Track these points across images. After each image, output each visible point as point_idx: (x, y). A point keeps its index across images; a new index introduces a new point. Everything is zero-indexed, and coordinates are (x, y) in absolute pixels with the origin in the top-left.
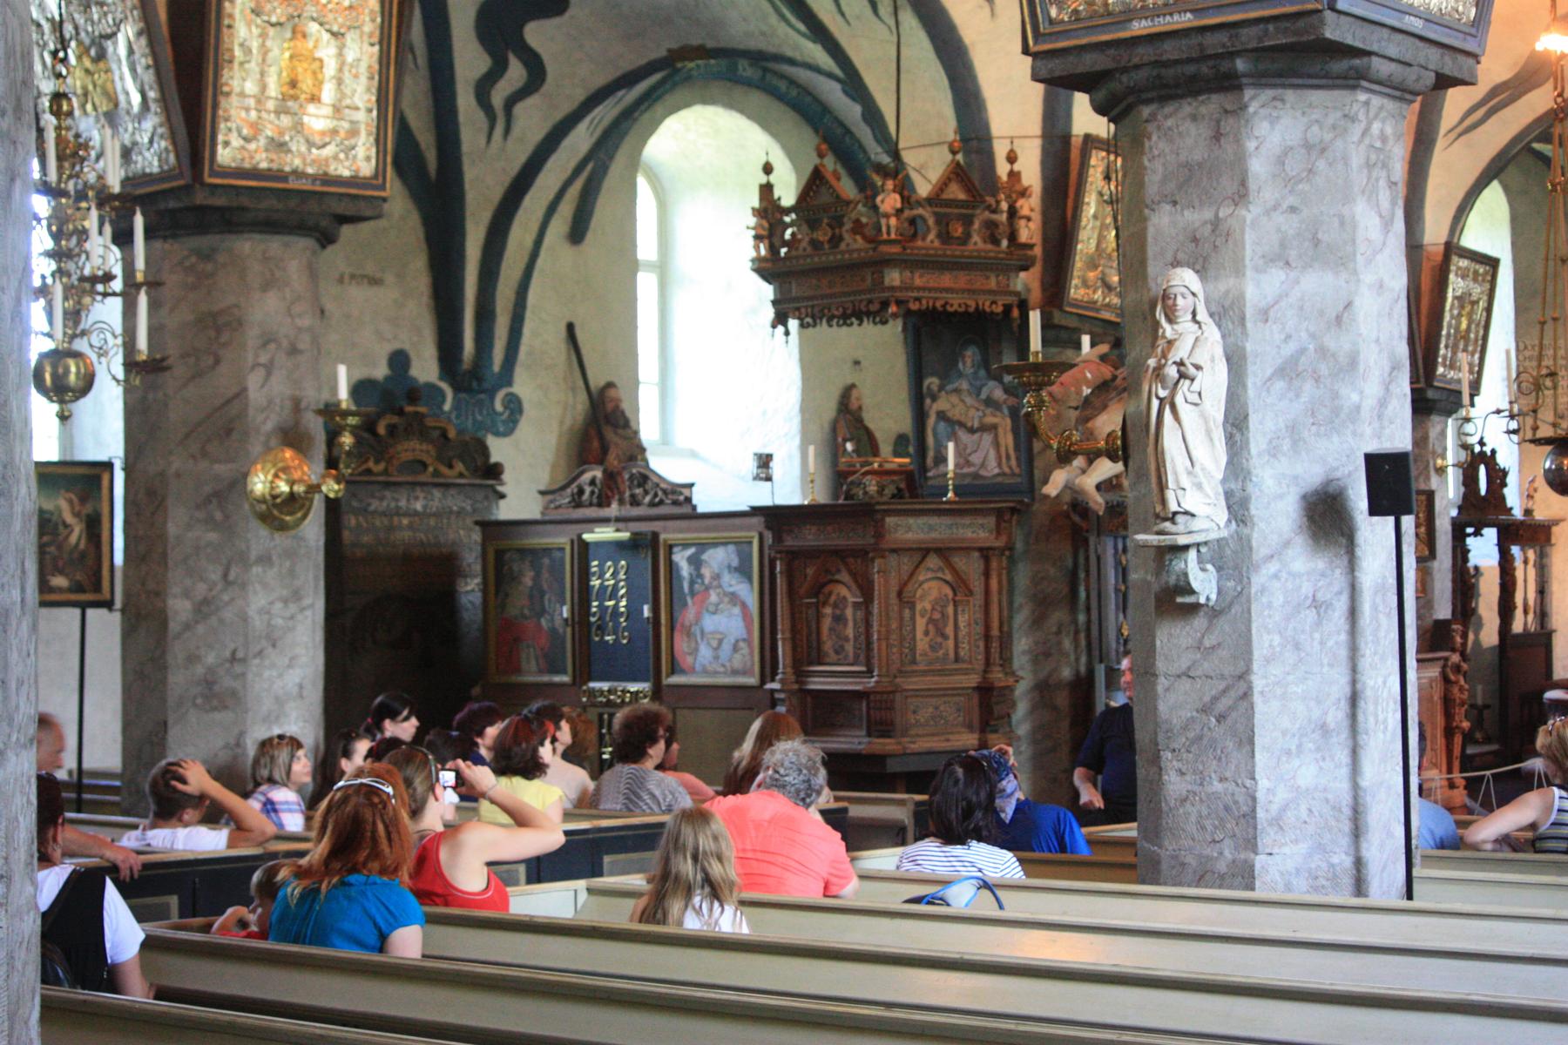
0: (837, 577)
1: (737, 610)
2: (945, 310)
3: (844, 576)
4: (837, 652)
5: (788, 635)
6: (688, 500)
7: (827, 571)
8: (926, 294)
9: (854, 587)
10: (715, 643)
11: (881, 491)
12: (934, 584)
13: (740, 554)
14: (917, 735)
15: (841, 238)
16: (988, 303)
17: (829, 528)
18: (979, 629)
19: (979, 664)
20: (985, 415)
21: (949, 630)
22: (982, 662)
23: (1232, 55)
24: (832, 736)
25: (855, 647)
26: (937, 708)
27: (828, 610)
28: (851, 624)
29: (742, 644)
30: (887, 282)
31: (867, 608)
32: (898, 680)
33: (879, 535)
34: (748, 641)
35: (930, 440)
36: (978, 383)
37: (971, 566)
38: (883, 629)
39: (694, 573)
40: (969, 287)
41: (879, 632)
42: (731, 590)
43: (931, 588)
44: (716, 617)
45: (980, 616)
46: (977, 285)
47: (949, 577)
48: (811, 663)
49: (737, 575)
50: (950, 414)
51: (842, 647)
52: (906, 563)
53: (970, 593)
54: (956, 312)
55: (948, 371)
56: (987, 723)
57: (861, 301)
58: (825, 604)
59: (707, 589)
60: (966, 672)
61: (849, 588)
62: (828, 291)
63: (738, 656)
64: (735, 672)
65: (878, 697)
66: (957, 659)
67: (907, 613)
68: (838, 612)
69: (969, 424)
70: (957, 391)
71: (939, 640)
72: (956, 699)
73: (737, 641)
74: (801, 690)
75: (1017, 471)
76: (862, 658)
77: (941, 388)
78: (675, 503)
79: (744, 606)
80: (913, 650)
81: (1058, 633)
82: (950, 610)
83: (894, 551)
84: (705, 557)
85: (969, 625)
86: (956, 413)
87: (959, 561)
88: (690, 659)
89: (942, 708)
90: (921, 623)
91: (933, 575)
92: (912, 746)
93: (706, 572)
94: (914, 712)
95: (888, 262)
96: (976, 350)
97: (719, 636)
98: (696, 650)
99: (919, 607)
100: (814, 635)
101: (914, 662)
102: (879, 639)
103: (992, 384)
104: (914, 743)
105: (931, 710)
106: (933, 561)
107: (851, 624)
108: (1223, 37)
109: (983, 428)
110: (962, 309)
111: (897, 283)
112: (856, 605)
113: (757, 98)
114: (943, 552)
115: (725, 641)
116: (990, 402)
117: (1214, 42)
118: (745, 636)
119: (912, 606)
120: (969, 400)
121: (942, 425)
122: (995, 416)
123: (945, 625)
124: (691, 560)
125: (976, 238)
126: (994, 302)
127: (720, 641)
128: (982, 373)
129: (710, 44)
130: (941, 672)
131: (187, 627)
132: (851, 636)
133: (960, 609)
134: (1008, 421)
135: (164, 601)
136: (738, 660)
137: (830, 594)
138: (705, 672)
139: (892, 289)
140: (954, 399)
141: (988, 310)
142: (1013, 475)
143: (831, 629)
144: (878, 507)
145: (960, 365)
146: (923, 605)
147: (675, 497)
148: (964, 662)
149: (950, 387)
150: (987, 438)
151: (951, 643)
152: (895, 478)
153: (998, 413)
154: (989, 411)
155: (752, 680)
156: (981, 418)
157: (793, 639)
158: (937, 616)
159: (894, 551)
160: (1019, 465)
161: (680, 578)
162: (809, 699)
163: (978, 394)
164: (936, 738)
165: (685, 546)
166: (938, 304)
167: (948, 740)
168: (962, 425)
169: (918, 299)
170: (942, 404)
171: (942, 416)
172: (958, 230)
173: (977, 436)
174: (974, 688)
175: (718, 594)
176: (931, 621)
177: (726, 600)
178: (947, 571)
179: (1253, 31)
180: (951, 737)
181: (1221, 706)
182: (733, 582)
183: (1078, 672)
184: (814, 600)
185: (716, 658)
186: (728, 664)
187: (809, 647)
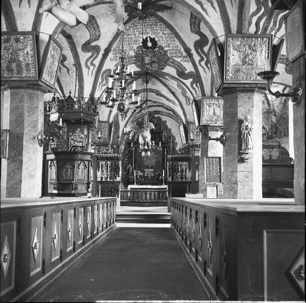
3: (69, 164)
23: (255, 87)
33: (77, 157)
35: (70, 143)
37: (86, 163)
43: (82, 166)
52: (79, 162)
55: (74, 132)
95: (82, 112)
108: (255, 85)
109: (80, 142)
112: (71, 169)
114: (84, 161)
116: (81, 137)
117: (253, 85)
121: (72, 141)
131: (26, 162)
135: (22, 157)
146: (81, 169)
150: (81, 143)
168: (76, 141)
170: (72, 137)
171: (72, 139)
179: (260, 85)
181: (248, 176)
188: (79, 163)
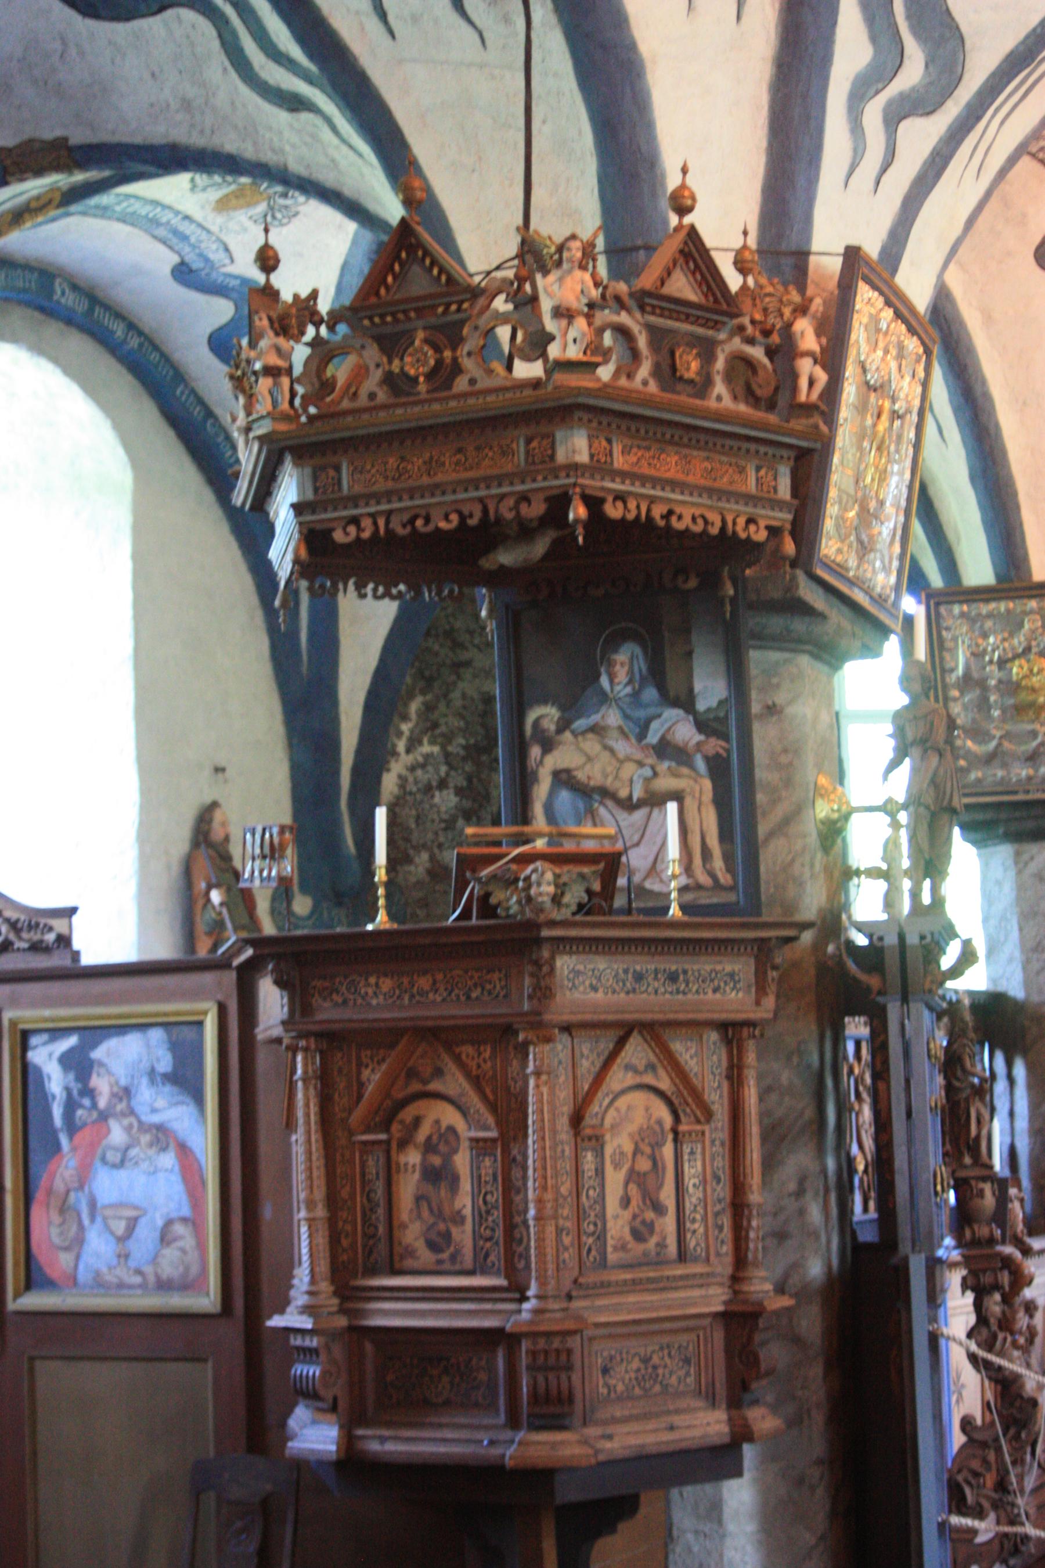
0: (434, 1086)
1: (168, 1160)
2: (668, 527)
3: (454, 1082)
4: (433, 1246)
5: (321, 1212)
6: (64, 941)
7: (412, 1074)
8: (638, 489)
9: (474, 1101)
10: (120, 1227)
11: (556, 900)
12: (639, 1099)
13: (174, 1047)
14: (615, 1421)
15: (457, 369)
16: (741, 521)
17: (424, 982)
18: (723, 1191)
19: (724, 1267)
20: (655, 774)
21: (667, 1195)
22: (729, 1259)
24: (422, 1425)
25: (476, 1236)
26: (646, 1360)
27: (413, 1157)
28: (466, 1185)
29: (179, 1229)
30: (561, 457)
31: (506, 1151)
32: (576, 1304)
33: (544, 992)
34: (195, 1222)
36: (641, 714)
38: (549, 1196)
39: (75, 1087)
40: (708, 483)
41: (539, 1201)
42: (156, 1119)
44: (122, 1174)
45: (722, 1163)
46: (723, 483)
47: (664, 1084)
48: (373, 1271)
49: (168, 1088)
50: (581, 776)
51: (447, 1236)
53: (709, 1115)
54: (687, 530)
56: (745, 1387)
57: (502, 497)
58: (404, 1144)
59: (104, 1117)
60: (703, 1281)
61: (464, 1111)
62: (425, 480)
63: (170, 1254)
64: (164, 1285)
65: (542, 1343)
66: (682, 1256)
67: (589, 1159)
68: (436, 1161)
69: (623, 793)
70: (596, 730)
71: (650, 1215)
72: (683, 1339)
73: (169, 1223)
74: (352, 1329)
75: (725, 878)
76: (496, 1257)
77: (563, 725)
78: (36, 947)
79: (184, 1150)
80: (601, 1237)
81: (800, 1193)
82: (668, 1151)
83: (567, 1028)
84: (98, 1054)
85: (704, 1182)
86: (593, 774)
87: (684, 1050)
88: (65, 1259)
89: (656, 1360)
90: (615, 1180)
91: (638, 1080)
92: (608, 1445)
93: (101, 1084)
94: (605, 1371)
96: (638, 650)
97: (131, 1213)
98: (79, 1241)
99: (608, 1150)
100: (381, 1211)
101: (603, 1263)
102: (538, 1218)
103: (672, 714)
104: (610, 1437)
105: (636, 1364)
106: (636, 1051)
107: (466, 1185)
110: (698, 528)
111: (583, 457)
113: (78, 343)
115: (143, 1221)
116: (665, 749)
118: (186, 1211)
119: (597, 1142)
120: (622, 747)
122: (677, 775)
123: (660, 1187)
124: (66, 1060)
125: (720, 388)
126: (750, 521)
127: (132, 1224)
128: (651, 693)
129: (78, 137)
130: (635, 1286)
132: (468, 1211)
133: (686, 1149)
134: (707, 784)
136: (170, 1262)
137: (417, 1121)
138: (99, 1283)
139: (574, 468)
140: (591, 745)
141: (743, 535)
142: (717, 885)
143: (418, 1199)
144: (545, 933)
145: (604, 681)
147: (36, 936)
148: (696, 1259)
149: (580, 724)
151: (669, 1223)
152: (586, 870)
153: (685, 771)
154: (664, 766)
155: (208, 1300)
156: (647, 780)
157: (332, 1221)
158: (644, 1165)
159: (567, 1028)
160: (730, 868)
161: (46, 1099)
162: (369, 1347)
163: (641, 736)
164: (651, 1426)
165: (56, 1033)
166: (658, 511)
167: (672, 1428)
168: (605, 793)
169: (620, 497)
171: (563, 778)
172: (691, 366)
173: (639, 815)
174: (716, 1315)
175: (129, 1129)
176: (633, 1176)
177: (145, 1139)
178: (661, 1072)
180: (677, 1420)
182: (160, 1103)
183: (829, 1267)
184: (383, 1137)
185: (124, 1256)
186: (148, 1270)
187: (370, 1236)
188: (588, 1066)
